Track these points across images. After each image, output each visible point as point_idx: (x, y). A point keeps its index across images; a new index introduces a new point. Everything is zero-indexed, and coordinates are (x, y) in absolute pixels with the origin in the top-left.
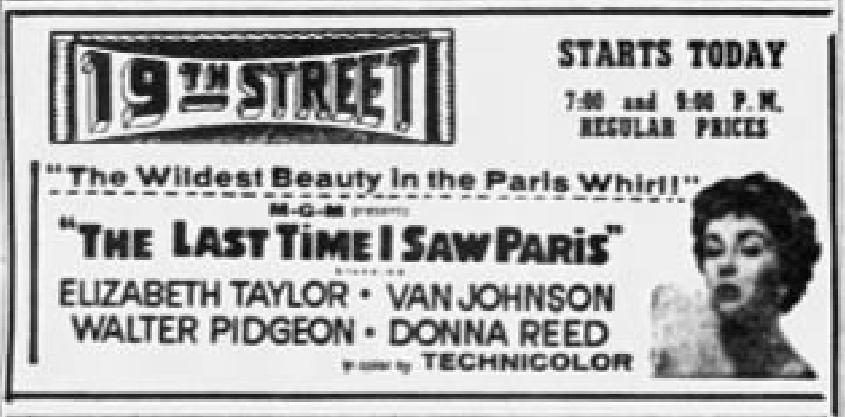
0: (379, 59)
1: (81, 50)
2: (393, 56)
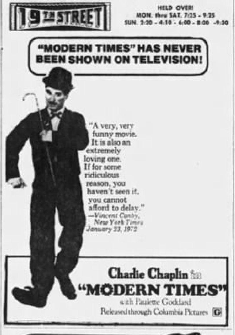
0: (92, 10)
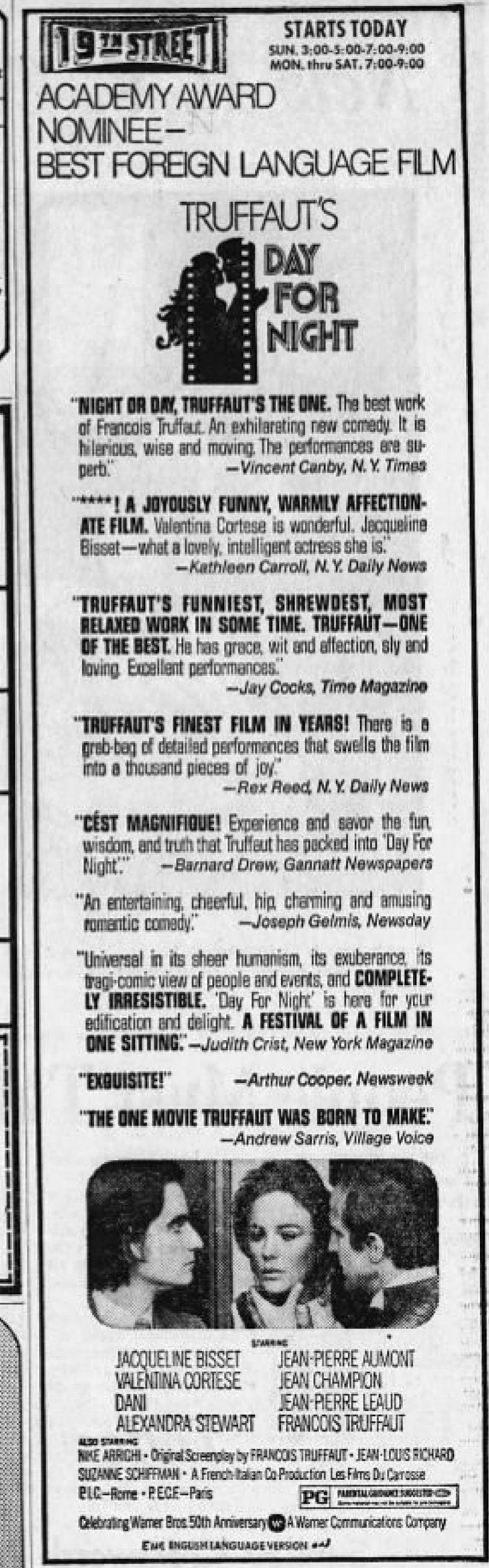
0: (190, 31)
1: (55, 26)
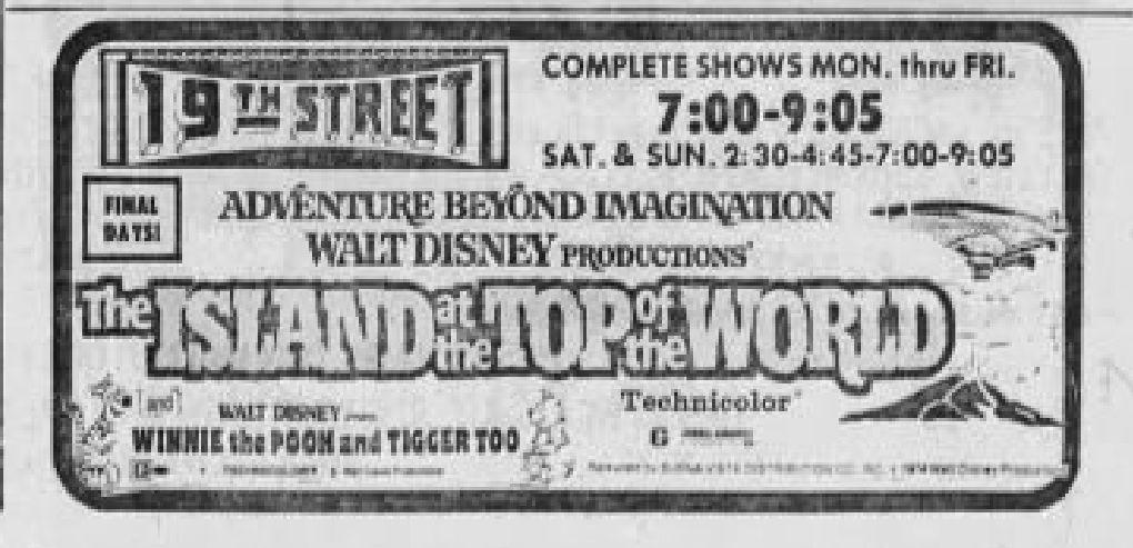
0: (433, 80)
2: (449, 77)
